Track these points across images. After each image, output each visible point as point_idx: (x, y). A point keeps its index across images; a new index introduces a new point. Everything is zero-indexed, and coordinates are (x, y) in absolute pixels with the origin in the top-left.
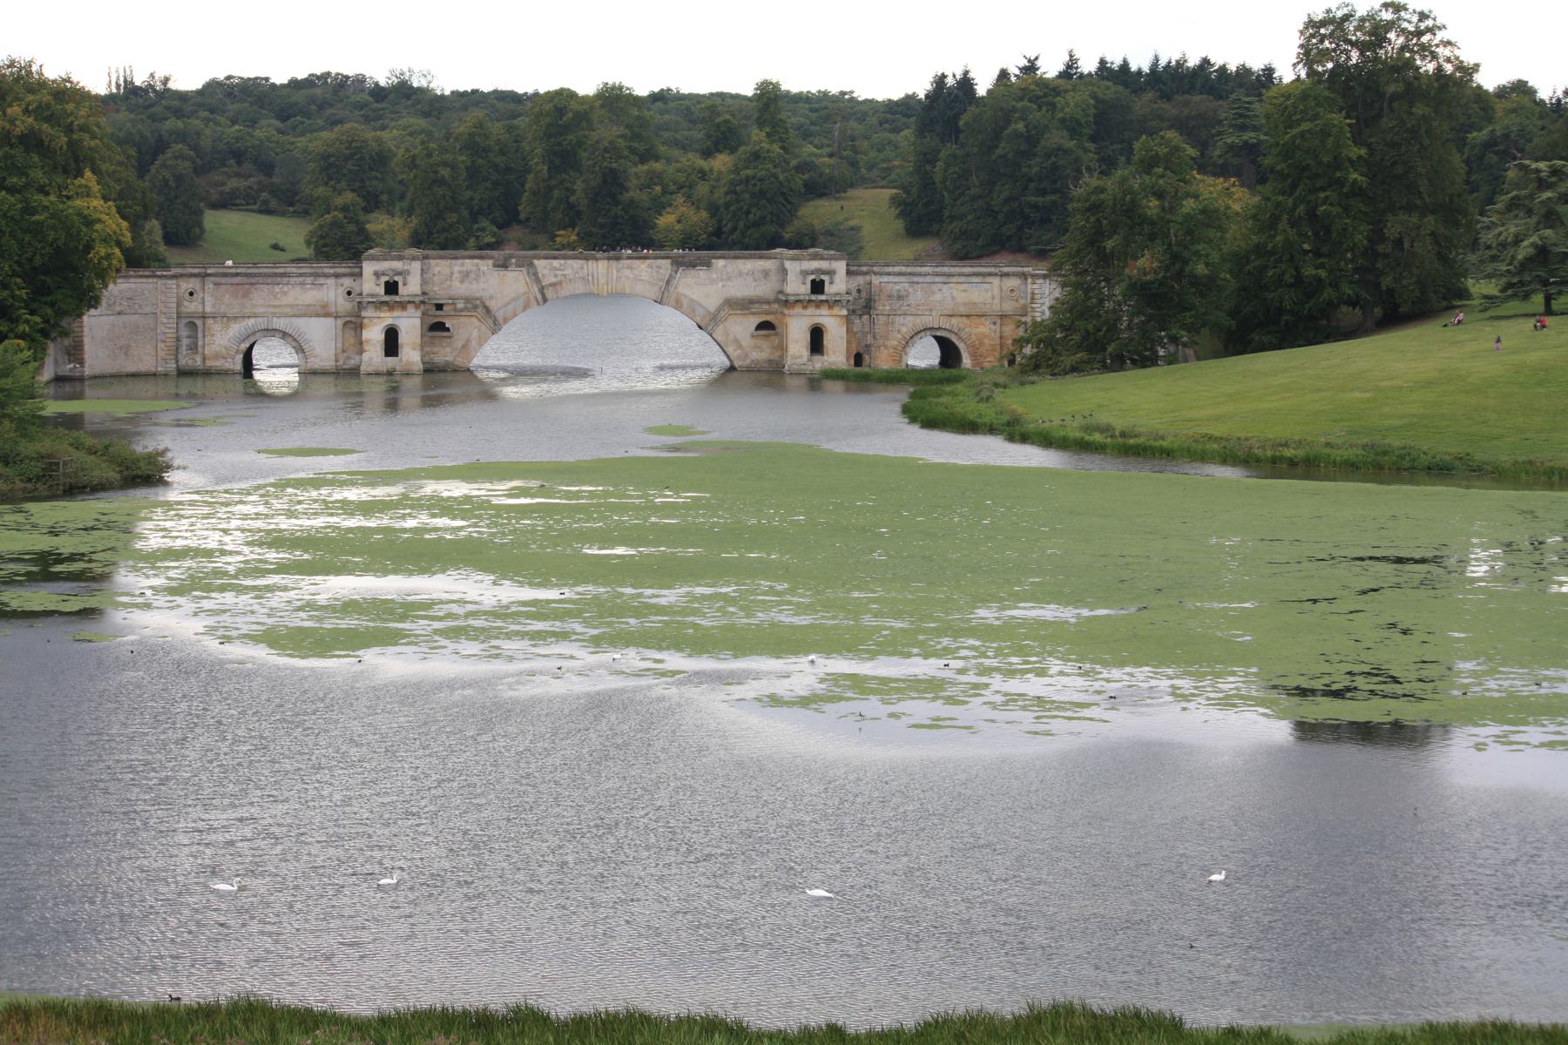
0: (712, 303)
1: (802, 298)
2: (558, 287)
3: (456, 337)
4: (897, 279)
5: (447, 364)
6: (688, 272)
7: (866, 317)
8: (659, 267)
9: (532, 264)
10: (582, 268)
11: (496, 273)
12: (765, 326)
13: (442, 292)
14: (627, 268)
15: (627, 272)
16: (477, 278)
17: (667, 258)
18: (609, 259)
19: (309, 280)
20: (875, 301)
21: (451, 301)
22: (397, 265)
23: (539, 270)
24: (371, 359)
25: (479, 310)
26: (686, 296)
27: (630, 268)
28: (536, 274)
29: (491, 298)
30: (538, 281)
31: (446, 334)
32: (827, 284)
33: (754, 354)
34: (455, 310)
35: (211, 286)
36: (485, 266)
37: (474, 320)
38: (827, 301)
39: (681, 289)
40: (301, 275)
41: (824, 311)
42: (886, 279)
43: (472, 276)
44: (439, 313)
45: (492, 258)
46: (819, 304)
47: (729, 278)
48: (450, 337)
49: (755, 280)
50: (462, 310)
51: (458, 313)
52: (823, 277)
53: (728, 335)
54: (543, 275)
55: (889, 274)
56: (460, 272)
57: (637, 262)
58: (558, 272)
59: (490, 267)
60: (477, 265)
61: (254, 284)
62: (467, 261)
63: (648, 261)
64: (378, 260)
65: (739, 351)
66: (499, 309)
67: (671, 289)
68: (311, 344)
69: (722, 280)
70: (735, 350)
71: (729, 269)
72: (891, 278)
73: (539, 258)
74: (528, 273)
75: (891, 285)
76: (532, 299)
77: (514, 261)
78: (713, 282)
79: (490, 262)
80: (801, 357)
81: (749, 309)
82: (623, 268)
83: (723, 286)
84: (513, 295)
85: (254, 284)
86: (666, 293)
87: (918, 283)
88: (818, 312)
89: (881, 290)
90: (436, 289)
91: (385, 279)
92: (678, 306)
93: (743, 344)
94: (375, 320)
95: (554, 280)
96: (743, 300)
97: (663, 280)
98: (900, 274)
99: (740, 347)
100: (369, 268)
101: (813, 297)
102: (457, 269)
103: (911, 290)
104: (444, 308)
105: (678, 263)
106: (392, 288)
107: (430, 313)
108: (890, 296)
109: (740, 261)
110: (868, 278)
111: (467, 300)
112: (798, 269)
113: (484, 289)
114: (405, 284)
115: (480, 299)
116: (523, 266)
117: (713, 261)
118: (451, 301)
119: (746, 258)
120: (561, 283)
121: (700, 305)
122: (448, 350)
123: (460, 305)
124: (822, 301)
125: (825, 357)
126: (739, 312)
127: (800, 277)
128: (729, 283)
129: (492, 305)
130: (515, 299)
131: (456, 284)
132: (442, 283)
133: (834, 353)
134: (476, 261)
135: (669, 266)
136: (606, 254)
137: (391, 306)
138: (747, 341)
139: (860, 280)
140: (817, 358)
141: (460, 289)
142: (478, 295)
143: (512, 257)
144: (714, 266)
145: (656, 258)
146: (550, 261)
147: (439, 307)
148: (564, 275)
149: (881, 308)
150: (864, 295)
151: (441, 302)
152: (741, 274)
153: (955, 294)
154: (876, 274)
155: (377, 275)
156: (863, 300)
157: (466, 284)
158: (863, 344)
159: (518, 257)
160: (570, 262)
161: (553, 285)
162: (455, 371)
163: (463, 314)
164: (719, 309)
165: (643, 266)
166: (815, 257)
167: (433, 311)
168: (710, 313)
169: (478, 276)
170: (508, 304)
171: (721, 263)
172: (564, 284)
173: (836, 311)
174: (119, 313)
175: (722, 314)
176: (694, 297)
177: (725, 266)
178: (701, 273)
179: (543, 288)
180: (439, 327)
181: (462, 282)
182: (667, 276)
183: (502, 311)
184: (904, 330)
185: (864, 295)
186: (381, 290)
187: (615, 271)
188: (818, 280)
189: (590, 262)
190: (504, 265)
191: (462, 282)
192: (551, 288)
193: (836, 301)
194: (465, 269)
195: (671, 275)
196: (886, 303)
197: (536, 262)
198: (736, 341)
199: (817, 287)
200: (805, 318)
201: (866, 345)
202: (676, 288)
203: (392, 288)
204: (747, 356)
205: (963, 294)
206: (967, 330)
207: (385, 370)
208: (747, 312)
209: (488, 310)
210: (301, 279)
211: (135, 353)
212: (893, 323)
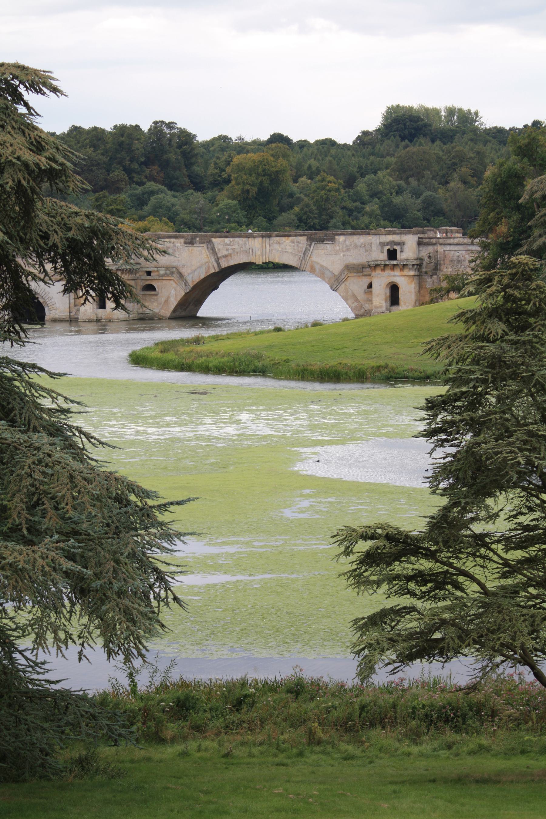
1: (379, 263)
2: (229, 258)
3: (160, 295)
4: (456, 248)
5: (155, 314)
6: (319, 245)
7: (435, 277)
8: (298, 242)
9: (210, 242)
10: (245, 244)
11: (187, 248)
14: (277, 243)
15: (276, 246)
17: (304, 235)
18: (263, 237)
20: (440, 265)
21: (156, 269)
23: (216, 246)
24: (86, 310)
25: (175, 275)
26: (318, 264)
28: (213, 249)
30: (215, 253)
31: (153, 293)
33: (367, 305)
34: (159, 276)
36: (179, 243)
37: (172, 282)
38: (397, 265)
39: (314, 258)
41: (397, 272)
42: (448, 248)
44: (148, 277)
45: (183, 237)
47: (348, 250)
48: (156, 295)
50: (163, 276)
51: (161, 278)
52: (395, 247)
53: (347, 292)
54: (219, 250)
55: (450, 244)
57: (283, 239)
63: (291, 238)
65: (356, 304)
66: (189, 274)
68: (53, 300)
69: (343, 251)
71: (348, 243)
73: (215, 237)
75: (452, 253)
76: (211, 266)
77: (198, 239)
78: (336, 252)
79: (182, 240)
80: (381, 307)
81: (362, 272)
82: (273, 243)
83: (344, 255)
84: (198, 264)
86: (303, 261)
88: (392, 273)
89: (445, 257)
92: (313, 270)
93: (359, 298)
95: (226, 253)
96: (358, 265)
97: (301, 252)
98: (458, 244)
99: (357, 300)
104: (152, 274)
105: (311, 240)
107: (142, 278)
108: (452, 261)
109: (355, 237)
110: (436, 247)
111: (167, 268)
112: (378, 241)
115: (176, 267)
116: (204, 243)
117: (337, 237)
118: (156, 269)
119: (360, 235)
120: (230, 255)
121: (328, 270)
122: (155, 304)
123: (162, 272)
124: (394, 265)
126: (355, 274)
127: (380, 247)
128: (348, 253)
129: (184, 271)
130: (200, 267)
133: (405, 304)
135: (305, 241)
136: (260, 233)
138: (361, 296)
139: (430, 249)
140: (394, 308)
142: (174, 264)
143: (197, 237)
145: (296, 236)
147: (149, 273)
148: (233, 249)
149: (445, 270)
150: (433, 260)
152: (356, 246)
154: (441, 244)
156: (433, 264)
159: (201, 237)
160: (237, 239)
161: (225, 256)
162: (160, 319)
163: (164, 278)
164: (341, 273)
165: (287, 242)
166: (389, 233)
167: (145, 277)
168: (335, 275)
170: (194, 271)
171: (342, 238)
173: (406, 272)
175: (343, 276)
176: (324, 264)
177: (345, 241)
178: (328, 247)
179: (218, 259)
180: (150, 288)
183: (191, 276)
185: (433, 260)
187: (268, 246)
188: (392, 249)
189: (250, 239)
190: (191, 243)
192: (224, 259)
193: (404, 265)
195: (306, 248)
196: (449, 266)
197: (213, 240)
199: (392, 254)
200: (384, 278)
202: (310, 257)
204: (362, 307)
207: (95, 318)
208: (361, 274)
209: (181, 275)
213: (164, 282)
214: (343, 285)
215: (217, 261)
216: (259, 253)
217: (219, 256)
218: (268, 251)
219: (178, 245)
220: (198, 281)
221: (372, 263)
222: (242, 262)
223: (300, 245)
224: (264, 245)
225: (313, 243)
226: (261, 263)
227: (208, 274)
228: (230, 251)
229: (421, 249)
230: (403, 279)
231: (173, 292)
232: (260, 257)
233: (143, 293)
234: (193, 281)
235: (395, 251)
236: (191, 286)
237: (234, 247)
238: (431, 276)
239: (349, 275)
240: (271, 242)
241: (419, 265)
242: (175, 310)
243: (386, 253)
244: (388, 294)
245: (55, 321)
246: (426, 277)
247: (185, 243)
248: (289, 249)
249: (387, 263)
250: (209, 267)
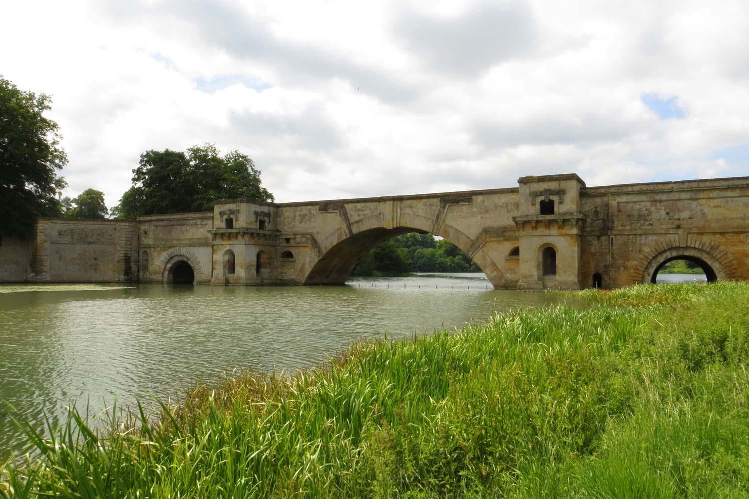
1: (530, 218)
6: (454, 207)
8: (431, 205)
10: (376, 209)
11: (321, 215)
13: (289, 230)
15: (408, 210)
16: (309, 220)
19: (199, 222)
21: (293, 236)
22: (232, 206)
23: (348, 212)
26: (452, 228)
27: (410, 207)
29: (318, 233)
31: (291, 259)
33: (509, 275)
35: (153, 227)
37: (307, 249)
38: (555, 221)
39: (449, 222)
40: (193, 219)
41: (554, 231)
43: (307, 218)
46: (549, 224)
47: (487, 211)
48: (293, 262)
52: (551, 197)
56: (300, 215)
58: (361, 213)
59: (318, 210)
60: (310, 211)
61: (172, 225)
62: (303, 207)
63: (423, 201)
64: (222, 204)
65: (495, 273)
70: (492, 272)
71: (486, 203)
72: (630, 198)
74: (340, 214)
75: (630, 206)
80: (531, 276)
83: (482, 218)
85: (172, 225)
86: (436, 226)
87: (661, 201)
88: (547, 232)
89: (619, 211)
90: (286, 228)
91: (225, 217)
93: (499, 267)
94: (220, 247)
95: (357, 218)
96: (499, 228)
100: (217, 209)
101: (541, 218)
102: (298, 213)
103: (653, 209)
104: (291, 241)
106: (229, 223)
107: (282, 245)
110: (605, 199)
112: (528, 191)
113: (314, 227)
114: (237, 220)
115: (311, 235)
117: (474, 197)
120: (362, 220)
122: (292, 270)
125: (557, 277)
126: (495, 239)
127: (530, 199)
129: (319, 238)
130: (333, 234)
131: (297, 223)
132: (289, 224)
133: (565, 272)
134: (309, 207)
135: (439, 203)
137: (230, 236)
138: (501, 264)
141: (300, 227)
142: (310, 231)
144: (474, 202)
146: (355, 204)
147: (288, 240)
148: (365, 215)
151: (288, 237)
152: (496, 207)
153: (706, 211)
155: (222, 214)
157: (303, 225)
158: (602, 265)
161: (358, 222)
164: (478, 238)
165: (419, 205)
167: (284, 244)
168: (472, 240)
169: (310, 218)
170: (327, 238)
172: (364, 222)
174: (90, 243)
177: (483, 201)
179: (350, 225)
180: (289, 255)
181: (301, 222)
182: (438, 211)
184: (646, 249)
185: (601, 216)
186: (223, 225)
187: (399, 210)
188: (547, 200)
189: (381, 204)
191: (301, 222)
194: (302, 213)
198: (493, 264)
199: (547, 207)
201: (605, 266)
203: (229, 223)
204: (502, 277)
205: (717, 210)
206: (722, 248)
210: (194, 221)
211: (102, 269)
213: (301, 249)
214: (480, 252)
215: (349, 226)
216: (389, 217)
217: (351, 222)
218: (399, 215)
219: (314, 212)
220: (330, 247)
221: (520, 219)
222: (373, 227)
223: (433, 208)
224: (395, 209)
225: (447, 206)
226: (391, 228)
227: (340, 241)
228: (361, 217)
229: (584, 202)
230: (562, 239)
231: (308, 259)
232: (391, 222)
233: (281, 259)
234: (326, 248)
235: (551, 203)
236: (325, 252)
237: (365, 212)
238: (599, 237)
239: (488, 240)
240: (403, 205)
241: (582, 222)
242: (310, 277)
243: (538, 206)
244: (541, 260)
245: (201, 283)
246: (591, 238)
247: (320, 210)
248: (421, 213)
249: (541, 218)
250: (341, 234)
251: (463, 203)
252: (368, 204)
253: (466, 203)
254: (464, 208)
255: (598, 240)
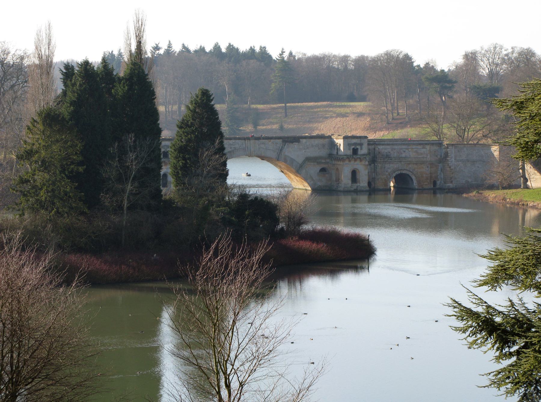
0: (300, 160)
8: (277, 143)
10: (243, 144)
12: (323, 170)
14: (263, 144)
15: (262, 146)
32: (359, 150)
33: (319, 183)
39: (286, 154)
41: (358, 162)
47: (308, 148)
49: (319, 149)
63: (272, 140)
65: (312, 182)
67: (283, 154)
69: (304, 149)
83: (305, 152)
93: (314, 179)
95: (230, 150)
99: (313, 180)
117: (301, 140)
148: (235, 147)
177: (306, 142)
199: (355, 151)
201: (373, 178)
206: (416, 170)
212: (384, 168)
223: (278, 145)
225: (287, 144)
243: (352, 151)
251: (296, 143)
252: (237, 141)
253: (297, 143)
254: (296, 145)
255: (370, 166)
